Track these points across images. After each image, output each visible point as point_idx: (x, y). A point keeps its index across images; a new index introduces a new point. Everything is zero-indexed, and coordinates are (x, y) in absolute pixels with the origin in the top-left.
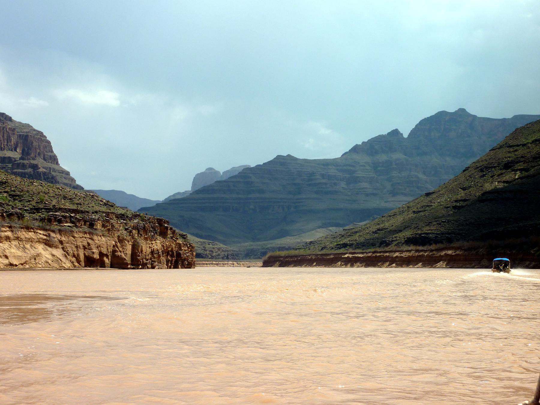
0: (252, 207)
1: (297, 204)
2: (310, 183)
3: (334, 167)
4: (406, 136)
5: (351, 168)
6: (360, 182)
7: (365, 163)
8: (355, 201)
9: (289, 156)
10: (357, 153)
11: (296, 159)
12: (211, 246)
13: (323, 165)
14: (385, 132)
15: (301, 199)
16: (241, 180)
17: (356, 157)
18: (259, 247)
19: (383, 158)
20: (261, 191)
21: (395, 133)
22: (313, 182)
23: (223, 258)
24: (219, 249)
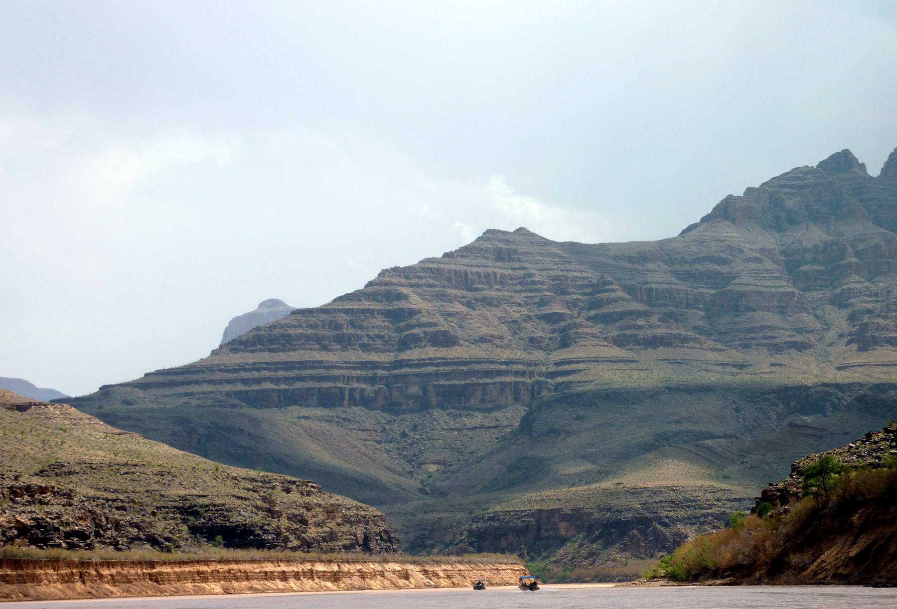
0: (414, 390)
1: (560, 379)
2: (593, 312)
3: (664, 267)
4: (874, 170)
5: (718, 268)
6: (748, 309)
7: (762, 250)
8: (742, 367)
9: (521, 231)
10: (733, 221)
11: (546, 243)
12: (295, 496)
13: (630, 259)
14: (812, 156)
15: (570, 362)
16: (378, 306)
17: (730, 233)
18: (459, 516)
19: (813, 235)
20: (444, 340)
21: (843, 161)
22: (605, 310)
23: (348, 548)
24: (331, 511)
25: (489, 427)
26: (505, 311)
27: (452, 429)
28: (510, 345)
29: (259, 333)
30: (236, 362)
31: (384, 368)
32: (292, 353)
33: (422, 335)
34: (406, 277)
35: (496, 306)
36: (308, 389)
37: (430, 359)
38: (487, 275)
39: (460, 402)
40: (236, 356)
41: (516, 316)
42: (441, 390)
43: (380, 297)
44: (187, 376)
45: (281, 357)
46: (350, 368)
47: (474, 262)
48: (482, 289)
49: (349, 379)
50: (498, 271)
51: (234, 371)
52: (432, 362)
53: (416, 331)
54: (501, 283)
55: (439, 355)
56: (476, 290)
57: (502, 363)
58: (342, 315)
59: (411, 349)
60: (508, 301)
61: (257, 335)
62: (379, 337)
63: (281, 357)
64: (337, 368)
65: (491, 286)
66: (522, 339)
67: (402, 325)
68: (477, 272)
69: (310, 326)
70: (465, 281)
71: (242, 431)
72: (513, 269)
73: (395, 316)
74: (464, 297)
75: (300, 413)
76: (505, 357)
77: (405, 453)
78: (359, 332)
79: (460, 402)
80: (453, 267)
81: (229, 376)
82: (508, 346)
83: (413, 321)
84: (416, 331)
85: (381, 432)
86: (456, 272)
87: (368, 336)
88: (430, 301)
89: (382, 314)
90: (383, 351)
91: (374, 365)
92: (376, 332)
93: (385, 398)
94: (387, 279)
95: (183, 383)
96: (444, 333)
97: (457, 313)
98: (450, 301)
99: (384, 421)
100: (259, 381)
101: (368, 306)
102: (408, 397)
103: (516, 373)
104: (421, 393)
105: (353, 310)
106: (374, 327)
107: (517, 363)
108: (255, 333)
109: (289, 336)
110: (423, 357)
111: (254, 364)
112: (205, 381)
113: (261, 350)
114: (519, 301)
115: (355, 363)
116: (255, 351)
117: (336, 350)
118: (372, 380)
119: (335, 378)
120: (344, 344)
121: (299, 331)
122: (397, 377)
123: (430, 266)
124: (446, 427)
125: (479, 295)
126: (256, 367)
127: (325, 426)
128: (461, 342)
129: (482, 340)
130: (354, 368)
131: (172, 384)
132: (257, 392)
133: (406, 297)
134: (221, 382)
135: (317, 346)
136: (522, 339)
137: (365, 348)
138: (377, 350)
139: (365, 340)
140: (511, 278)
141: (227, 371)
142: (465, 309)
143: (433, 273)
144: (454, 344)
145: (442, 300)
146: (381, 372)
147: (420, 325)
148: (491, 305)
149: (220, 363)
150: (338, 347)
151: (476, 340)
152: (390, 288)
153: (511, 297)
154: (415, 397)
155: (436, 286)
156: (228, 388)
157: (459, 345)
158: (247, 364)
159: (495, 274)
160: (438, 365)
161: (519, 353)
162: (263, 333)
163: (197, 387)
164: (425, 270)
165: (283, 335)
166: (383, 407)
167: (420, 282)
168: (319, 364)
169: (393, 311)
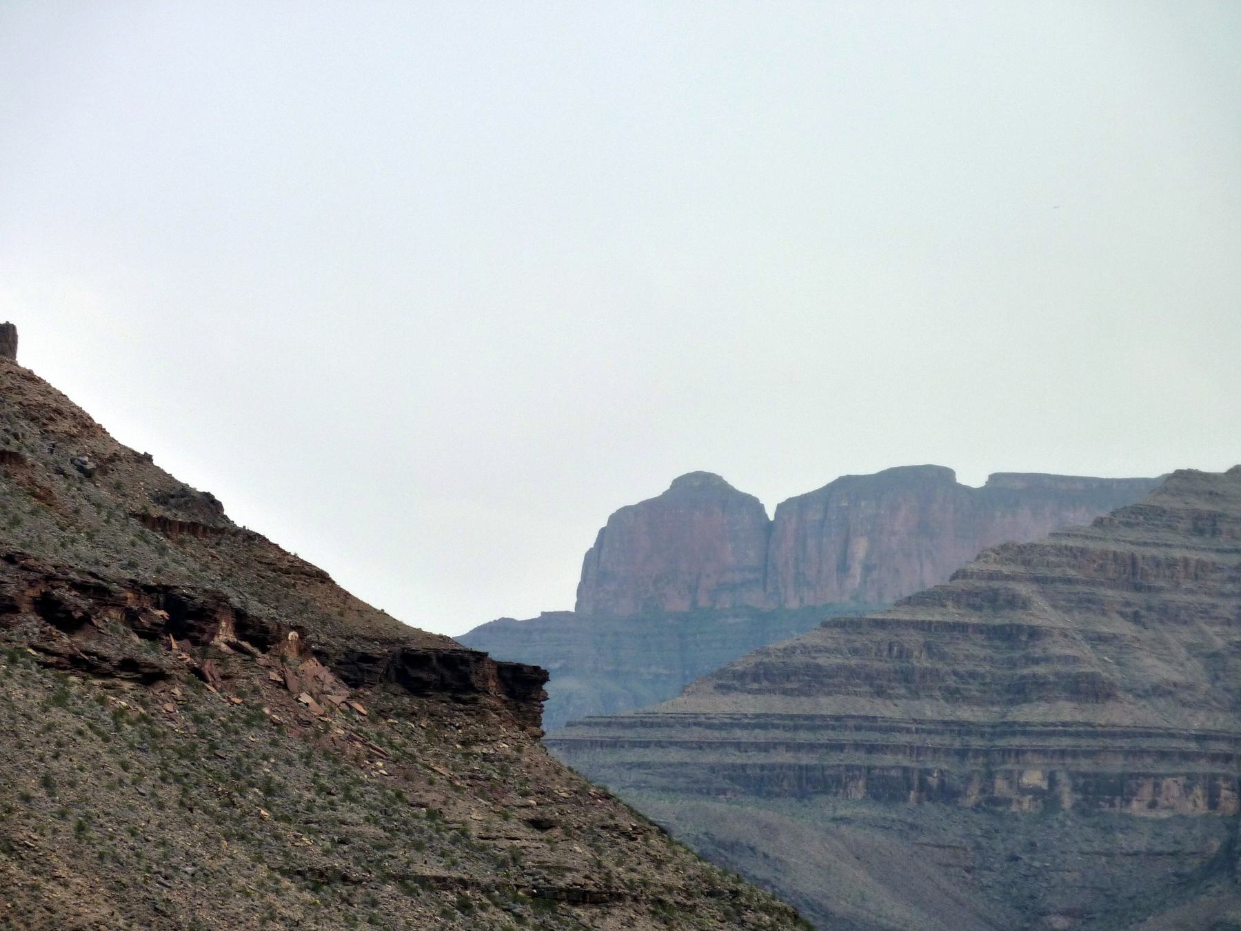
0: (1033, 778)
25: (1160, 854)
26: (1201, 632)
27: (1098, 853)
28: (1207, 702)
29: (766, 660)
30: (727, 710)
31: (982, 735)
32: (823, 700)
33: (1052, 678)
34: (1027, 563)
35: (1185, 623)
36: (849, 768)
37: (1064, 724)
38: (1172, 564)
39: (1112, 805)
40: (726, 699)
41: (1219, 643)
42: (1081, 781)
43: (978, 601)
44: (642, 731)
45: (802, 706)
46: (923, 731)
47: (1148, 537)
48: (1160, 590)
49: (917, 751)
50: (1193, 556)
51: (722, 727)
52: (1065, 730)
53: (1040, 670)
54: (1196, 577)
55: (1079, 717)
56: (1150, 589)
57: (1188, 738)
58: (912, 631)
59: (1031, 701)
60: (1206, 613)
61: (761, 663)
62: (973, 675)
63: (802, 706)
64: (900, 730)
65: (1178, 584)
66: (1227, 690)
67: (1017, 654)
68: (1153, 558)
69: (855, 651)
70: (1131, 573)
71: (752, 849)
72: (1218, 551)
73: (1007, 635)
74: (1128, 604)
75: (835, 809)
76: (1196, 725)
77: (1014, 891)
78: (940, 666)
79: (1112, 805)
80: (1112, 547)
81: (715, 735)
82: (1202, 705)
83: (1037, 652)
84: (1040, 670)
85: (973, 849)
86: (1115, 553)
87: (955, 673)
88: (1068, 611)
89: (981, 632)
90: (980, 703)
91: (963, 728)
92: (970, 666)
93: (983, 791)
94: (994, 567)
95: (634, 744)
96: (1092, 679)
97: (1115, 637)
98: (1104, 613)
99: (978, 833)
100: (765, 748)
101: (957, 618)
102: (1023, 791)
103: (1214, 758)
104: (1044, 785)
105: (930, 623)
106: (967, 657)
107: (1217, 739)
108: (759, 659)
109: (818, 667)
110: (1052, 719)
111: (758, 716)
112: (671, 743)
113: (769, 691)
114: (1227, 614)
115: (932, 722)
116: (760, 691)
117: (899, 697)
118: (962, 754)
119: (896, 749)
120: (913, 686)
121: (837, 660)
122: (1006, 752)
123: (1070, 543)
124: (1086, 848)
125: (1155, 601)
126: (762, 722)
127: (879, 837)
128: (1120, 694)
129: (1158, 691)
130: (930, 732)
131: (615, 744)
132: (763, 767)
133: (1025, 605)
134: (700, 746)
135: (866, 688)
136: (1227, 690)
137: (952, 695)
138: (968, 700)
139: (951, 682)
140: (1216, 568)
141: (710, 727)
142: (1125, 629)
143: (1075, 557)
144: (1109, 696)
145: (1088, 609)
146: (976, 743)
147: (1047, 660)
148: (1176, 618)
149: (698, 710)
150: (903, 691)
151: (1146, 691)
152: (996, 584)
153: (1214, 606)
154: (1036, 792)
155: (1077, 582)
156: (711, 758)
157: (1116, 698)
158: (746, 716)
159: (1186, 562)
160: (1077, 735)
161: (1222, 718)
162: (774, 659)
163: (660, 752)
164: (1060, 551)
165: (807, 666)
166: (978, 805)
167: (1049, 574)
168: (869, 722)
169: (1002, 627)
